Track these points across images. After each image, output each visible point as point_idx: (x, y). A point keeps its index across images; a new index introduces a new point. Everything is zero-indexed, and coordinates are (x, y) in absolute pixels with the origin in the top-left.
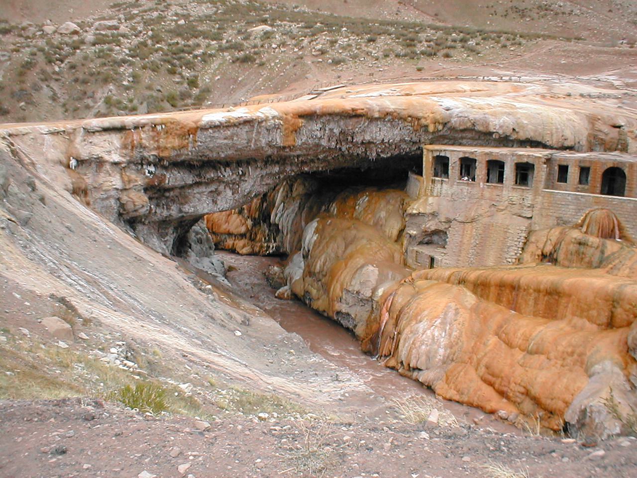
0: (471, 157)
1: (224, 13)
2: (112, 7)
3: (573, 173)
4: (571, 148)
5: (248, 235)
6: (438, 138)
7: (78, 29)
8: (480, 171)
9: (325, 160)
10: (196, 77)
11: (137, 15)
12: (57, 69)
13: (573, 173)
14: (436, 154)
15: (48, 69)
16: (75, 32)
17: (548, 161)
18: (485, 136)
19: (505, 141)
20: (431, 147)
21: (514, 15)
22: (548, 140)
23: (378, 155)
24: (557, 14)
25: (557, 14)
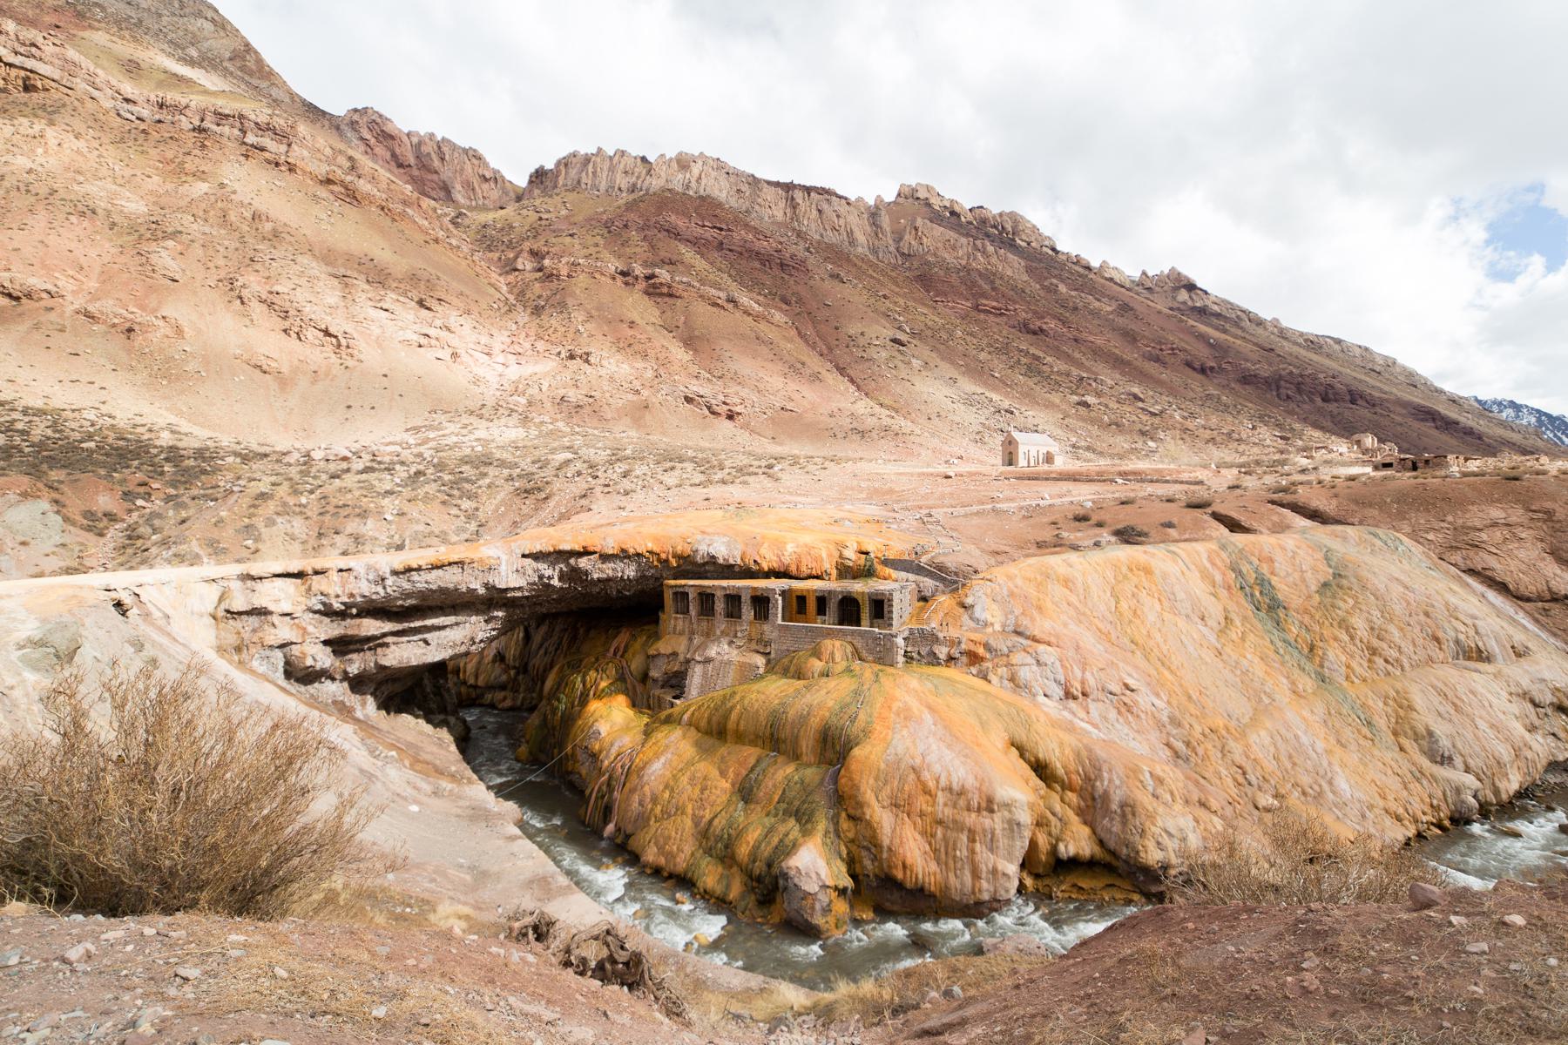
0: (709, 591)
1: (537, 437)
2: (407, 430)
3: (812, 605)
4: (817, 577)
5: (510, 686)
6: (680, 573)
7: (350, 455)
8: (720, 606)
9: (557, 601)
10: (477, 509)
11: (433, 439)
12: (304, 500)
13: (812, 605)
14: (675, 590)
15: (291, 501)
16: (345, 459)
17: (783, 593)
18: (728, 571)
19: (748, 573)
20: (672, 582)
21: (854, 437)
22: (793, 569)
23: (618, 591)
24: (897, 434)
25: (897, 434)
